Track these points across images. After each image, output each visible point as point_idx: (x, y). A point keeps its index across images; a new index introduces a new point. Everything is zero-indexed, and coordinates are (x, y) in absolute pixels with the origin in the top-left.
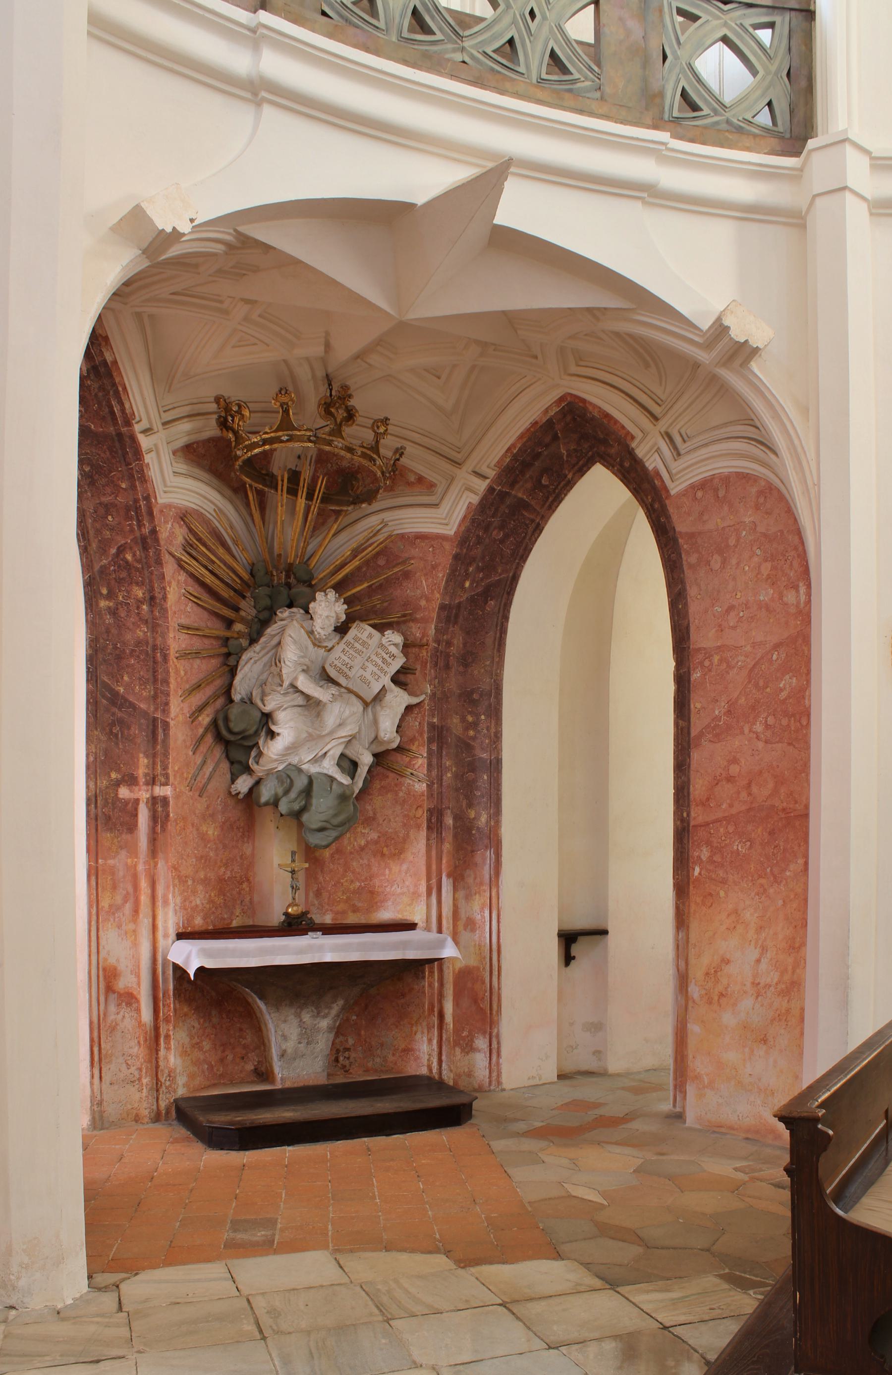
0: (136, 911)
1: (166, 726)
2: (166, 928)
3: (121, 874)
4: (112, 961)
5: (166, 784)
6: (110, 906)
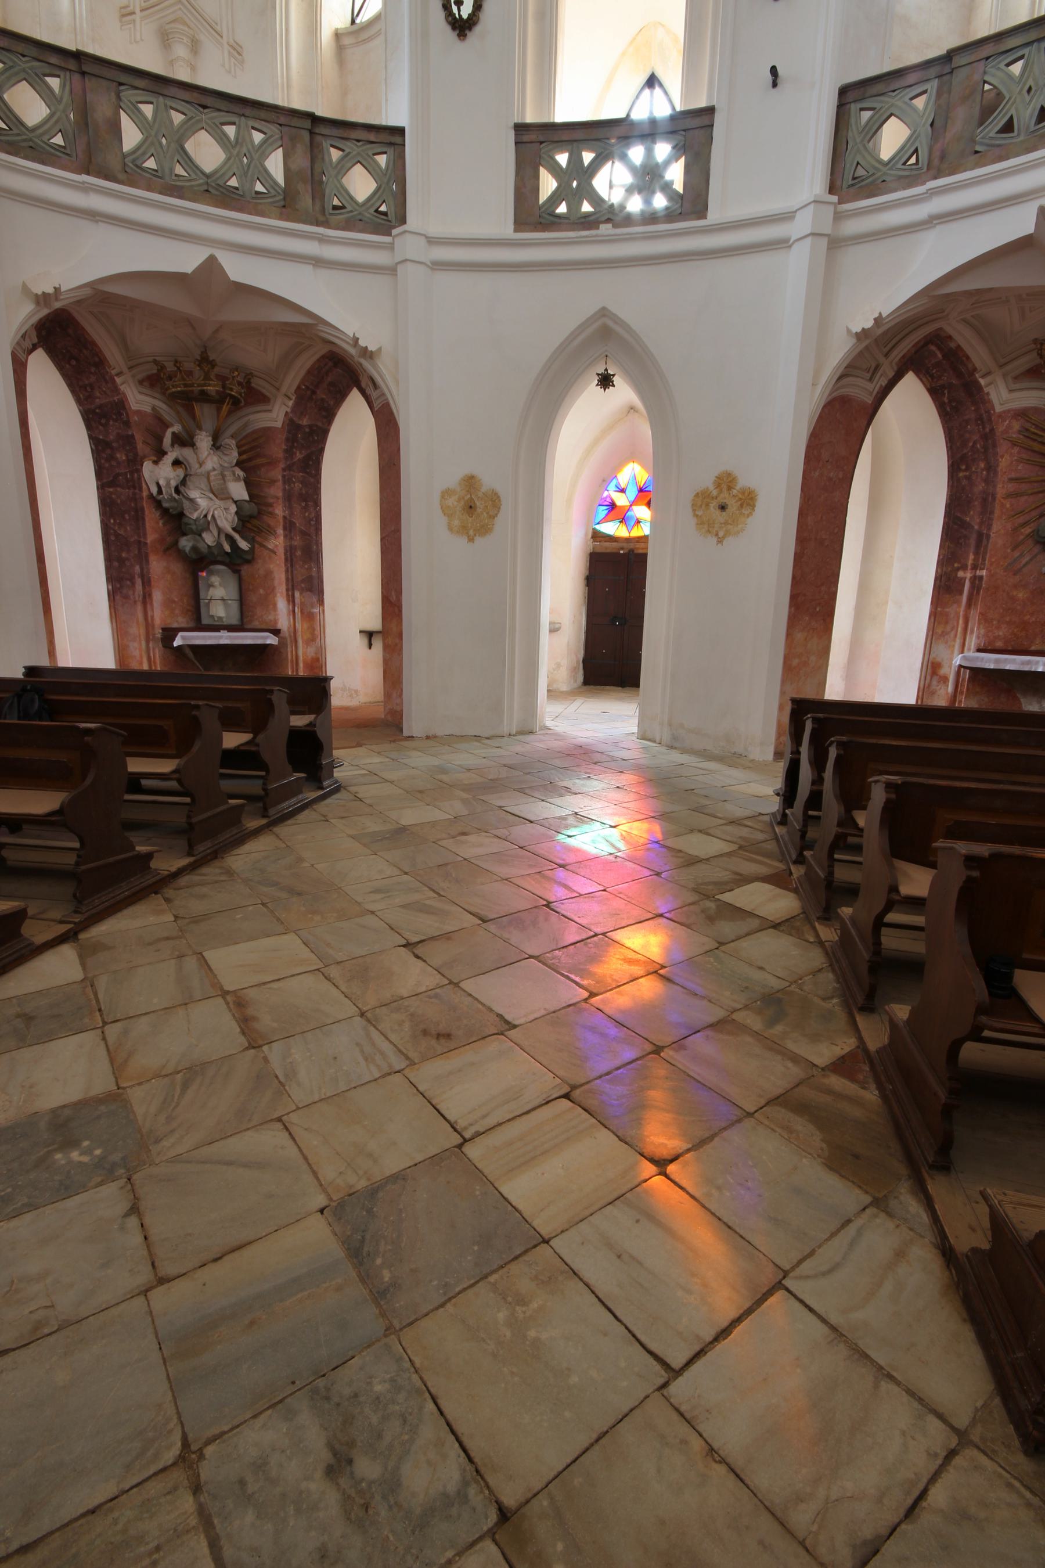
0: (956, 636)
1: (988, 536)
2: (970, 646)
3: (952, 616)
4: (939, 659)
5: (983, 569)
6: (943, 632)
